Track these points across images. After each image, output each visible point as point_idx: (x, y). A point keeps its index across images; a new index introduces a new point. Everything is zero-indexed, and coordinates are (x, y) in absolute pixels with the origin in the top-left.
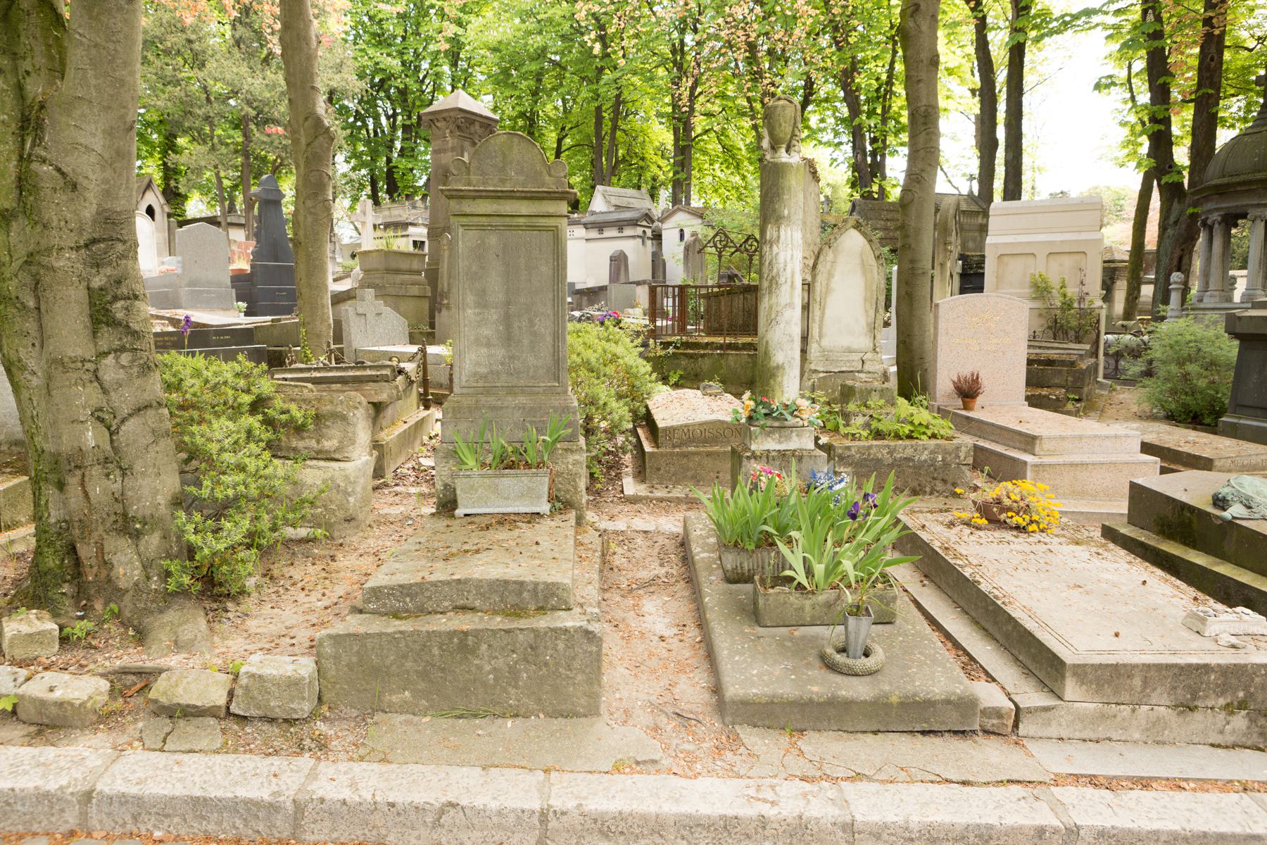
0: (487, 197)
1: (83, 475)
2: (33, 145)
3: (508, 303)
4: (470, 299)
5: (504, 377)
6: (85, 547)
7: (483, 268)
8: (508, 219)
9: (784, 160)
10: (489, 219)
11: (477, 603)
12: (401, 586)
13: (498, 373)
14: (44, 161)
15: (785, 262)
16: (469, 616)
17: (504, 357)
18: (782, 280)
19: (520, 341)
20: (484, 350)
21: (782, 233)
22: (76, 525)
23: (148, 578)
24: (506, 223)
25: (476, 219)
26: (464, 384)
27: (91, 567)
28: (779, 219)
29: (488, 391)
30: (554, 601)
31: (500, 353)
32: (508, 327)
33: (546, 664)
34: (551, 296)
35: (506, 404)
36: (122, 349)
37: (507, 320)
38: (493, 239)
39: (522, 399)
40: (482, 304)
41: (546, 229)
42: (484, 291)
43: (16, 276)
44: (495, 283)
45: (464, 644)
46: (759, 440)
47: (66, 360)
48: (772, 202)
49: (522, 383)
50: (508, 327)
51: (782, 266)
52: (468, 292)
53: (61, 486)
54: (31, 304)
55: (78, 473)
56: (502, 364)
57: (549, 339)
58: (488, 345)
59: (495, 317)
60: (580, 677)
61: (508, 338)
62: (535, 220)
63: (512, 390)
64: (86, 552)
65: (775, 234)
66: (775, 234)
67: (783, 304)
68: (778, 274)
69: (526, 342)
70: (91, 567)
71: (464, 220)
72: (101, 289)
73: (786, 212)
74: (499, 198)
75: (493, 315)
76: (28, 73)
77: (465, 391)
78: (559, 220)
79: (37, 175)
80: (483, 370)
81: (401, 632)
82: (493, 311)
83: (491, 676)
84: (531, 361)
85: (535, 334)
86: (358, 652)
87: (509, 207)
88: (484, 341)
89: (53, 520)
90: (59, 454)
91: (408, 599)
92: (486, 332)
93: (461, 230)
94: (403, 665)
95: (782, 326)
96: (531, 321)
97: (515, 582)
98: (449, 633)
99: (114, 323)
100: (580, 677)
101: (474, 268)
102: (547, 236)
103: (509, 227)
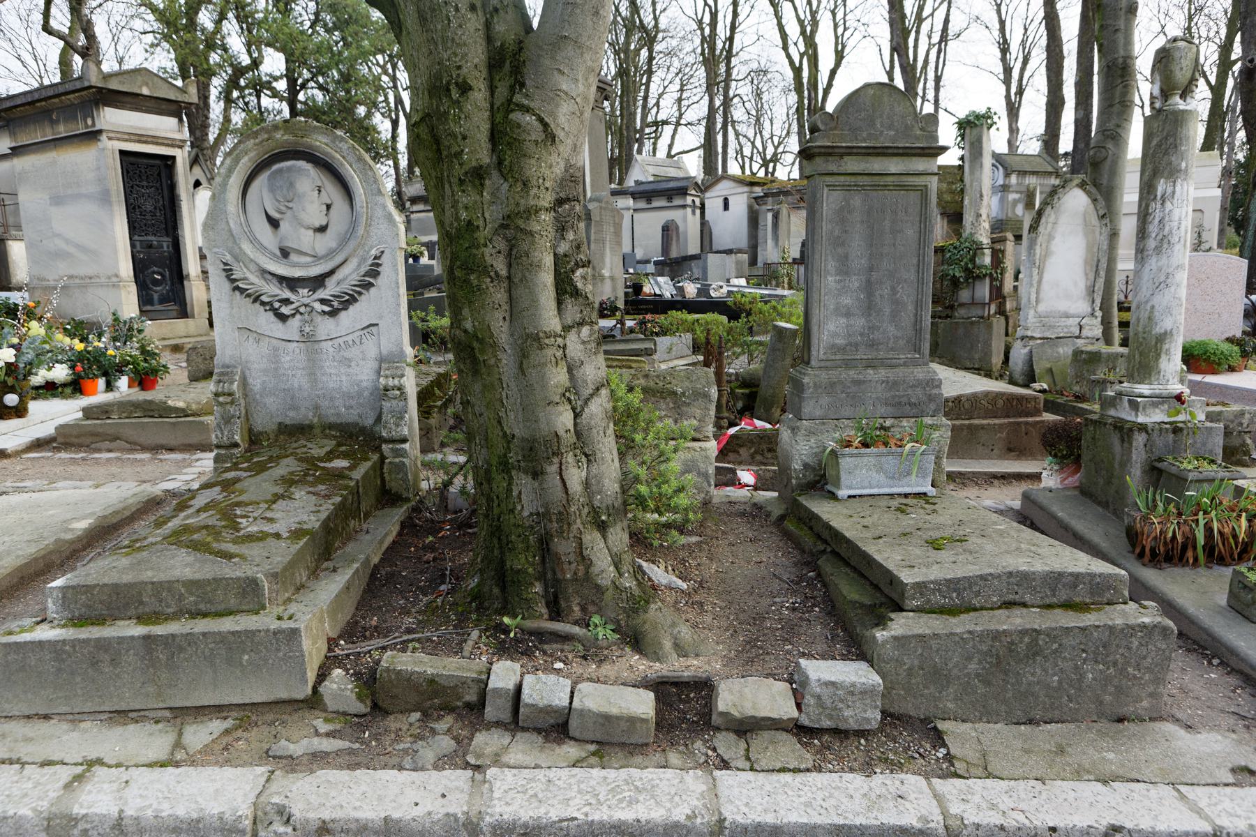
0: (857, 154)
1: (561, 464)
2: (512, 90)
3: (871, 269)
4: (831, 265)
5: (862, 348)
6: (564, 542)
7: (846, 232)
8: (876, 178)
9: (1181, 107)
10: (853, 179)
11: (1027, 598)
12: (949, 581)
13: (856, 345)
14: (527, 110)
15: (1180, 220)
16: (1018, 611)
17: (863, 327)
18: (1174, 239)
19: (880, 310)
20: (843, 320)
21: (1178, 188)
22: (554, 518)
23: (621, 575)
24: (877, 182)
25: (842, 178)
26: (821, 356)
27: (570, 563)
28: (1173, 173)
29: (848, 365)
30: (1108, 596)
31: (859, 322)
32: (870, 295)
33: (1115, 664)
34: (915, 262)
35: (869, 378)
36: (581, 324)
37: (869, 287)
38: (857, 201)
39: (883, 373)
40: (844, 270)
41: (913, 188)
42: (846, 257)
43: (490, 241)
44: (857, 247)
45: (1033, 646)
46: (1148, 411)
47: (541, 335)
48: (1166, 153)
49: (882, 355)
50: (870, 295)
51: (1176, 224)
52: (830, 258)
53: (537, 474)
54: (504, 273)
55: (556, 460)
56: (861, 335)
57: (911, 307)
58: (848, 315)
59: (857, 285)
60: (1147, 677)
61: (869, 307)
62: (904, 178)
63: (871, 364)
64: (563, 547)
65: (1169, 190)
66: (1169, 190)
67: (1175, 265)
68: (1171, 233)
69: (887, 311)
70: (570, 563)
71: (829, 180)
72: (566, 256)
73: (1184, 165)
74: (869, 154)
75: (855, 282)
76: (496, 10)
77: (822, 364)
78: (929, 178)
79: (519, 126)
80: (840, 342)
81: (970, 632)
82: (854, 278)
83: (1056, 678)
84: (892, 330)
85: (896, 302)
86: (921, 655)
87: (877, 165)
88: (844, 311)
89: (526, 514)
90: (535, 440)
91: (955, 595)
92: (847, 301)
93: (826, 190)
94: (966, 667)
95: (1172, 289)
96: (893, 289)
97: (1071, 574)
98: (1020, 632)
99: (576, 293)
100: (1147, 677)
101: (836, 233)
102: (914, 197)
103: (875, 187)
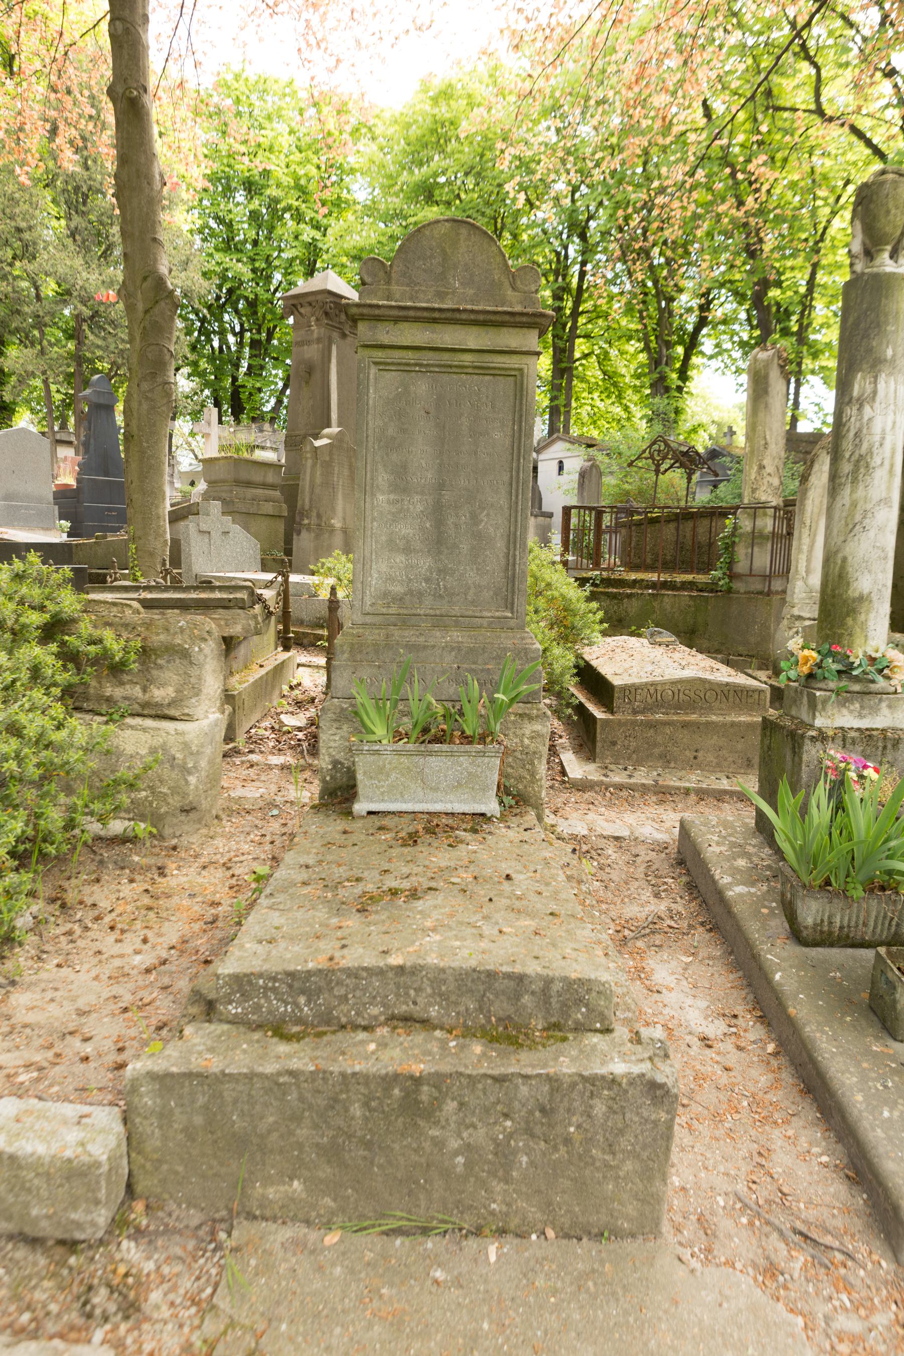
0: (416, 320)
3: (441, 486)
4: (383, 478)
5: (428, 601)
7: (404, 431)
8: (446, 356)
9: (888, 269)
11: (433, 1012)
12: (291, 975)
13: (420, 594)
15: (884, 432)
17: (430, 569)
18: (877, 460)
20: (400, 559)
21: (881, 386)
25: (397, 354)
26: (368, 609)
28: (876, 364)
29: (404, 621)
31: (425, 563)
32: (439, 523)
33: (567, 1141)
34: (506, 478)
35: (432, 642)
37: (438, 513)
38: (422, 387)
39: (456, 636)
40: (401, 485)
41: (504, 373)
44: (421, 456)
45: (411, 1100)
48: (866, 336)
49: (456, 610)
50: (439, 523)
51: (877, 438)
56: (428, 580)
57: (500, 544)
58: (407, 550)
59: (420, 508)
60: (629, 1166)
61: (438, 542)
62: (488, 358)
63: (440, 621)
65: (869, 388)
68: (870, 452)
69: (465, 547)
71: (379, 354)
73: (889, 352)
74: (435, 321)
75: (417, 505)
77: (369, 619)
80: (398, 589)
81: (291, 1073)
82: (417, 498)
83: (460, 1160)
84: (472, 576)
85: (478, 536)
86: (206, 1107)
87: (449, 336)
88: (401, 544)
91: (302, 1000)
92: (405, 529)
93: (373, 370)
94: (291, 1133)
95: (872, 534)
97: (509, 976)
98: (384, 1078)
100: (629, 1166)
101: (391, 432)
102: (504, 386)
103: (448, 368)
